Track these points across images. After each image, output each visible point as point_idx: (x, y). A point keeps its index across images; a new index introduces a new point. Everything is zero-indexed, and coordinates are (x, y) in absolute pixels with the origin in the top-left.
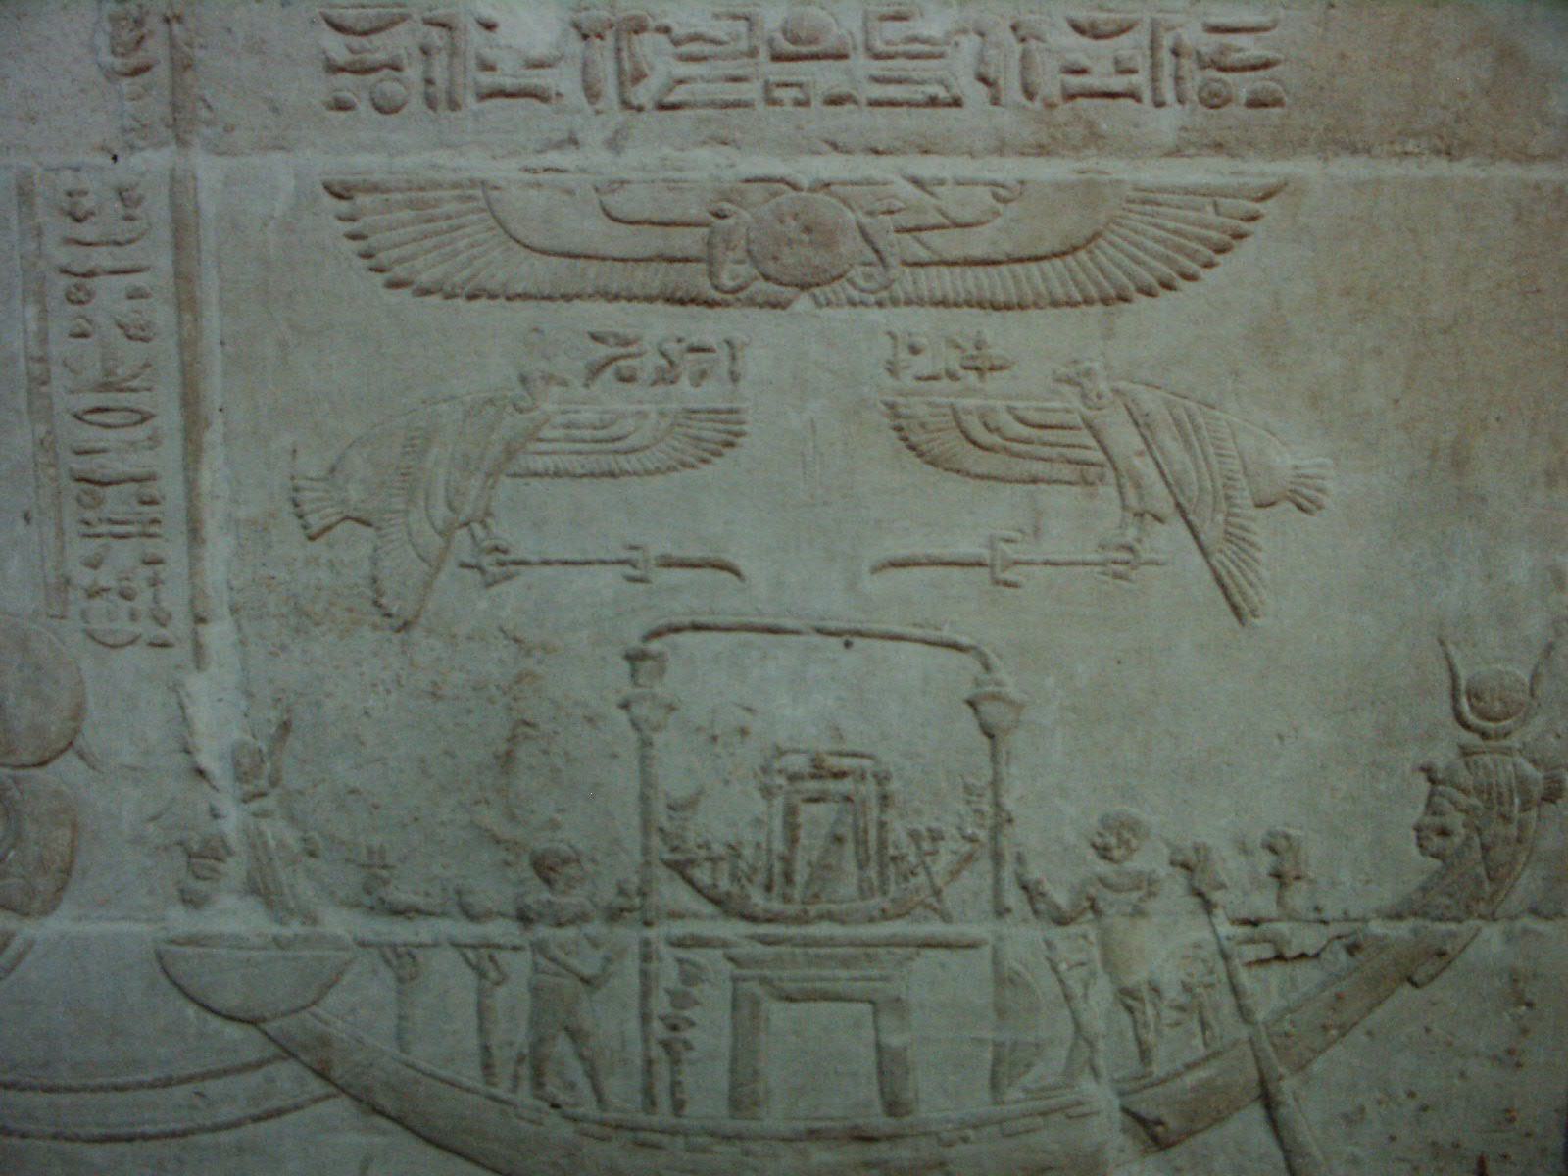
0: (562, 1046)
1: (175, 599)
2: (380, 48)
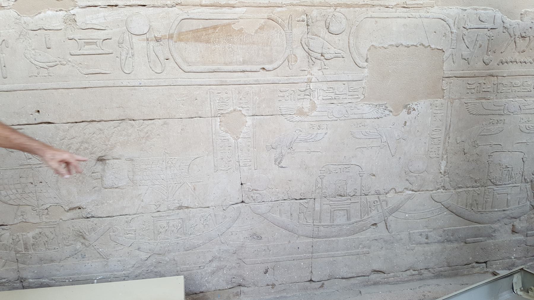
0: (475, 202)
1: (440, 152)
2: (473, 87)
